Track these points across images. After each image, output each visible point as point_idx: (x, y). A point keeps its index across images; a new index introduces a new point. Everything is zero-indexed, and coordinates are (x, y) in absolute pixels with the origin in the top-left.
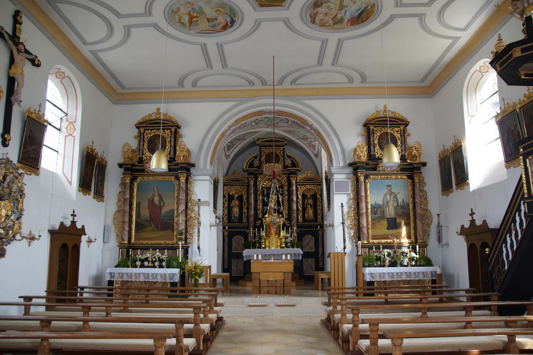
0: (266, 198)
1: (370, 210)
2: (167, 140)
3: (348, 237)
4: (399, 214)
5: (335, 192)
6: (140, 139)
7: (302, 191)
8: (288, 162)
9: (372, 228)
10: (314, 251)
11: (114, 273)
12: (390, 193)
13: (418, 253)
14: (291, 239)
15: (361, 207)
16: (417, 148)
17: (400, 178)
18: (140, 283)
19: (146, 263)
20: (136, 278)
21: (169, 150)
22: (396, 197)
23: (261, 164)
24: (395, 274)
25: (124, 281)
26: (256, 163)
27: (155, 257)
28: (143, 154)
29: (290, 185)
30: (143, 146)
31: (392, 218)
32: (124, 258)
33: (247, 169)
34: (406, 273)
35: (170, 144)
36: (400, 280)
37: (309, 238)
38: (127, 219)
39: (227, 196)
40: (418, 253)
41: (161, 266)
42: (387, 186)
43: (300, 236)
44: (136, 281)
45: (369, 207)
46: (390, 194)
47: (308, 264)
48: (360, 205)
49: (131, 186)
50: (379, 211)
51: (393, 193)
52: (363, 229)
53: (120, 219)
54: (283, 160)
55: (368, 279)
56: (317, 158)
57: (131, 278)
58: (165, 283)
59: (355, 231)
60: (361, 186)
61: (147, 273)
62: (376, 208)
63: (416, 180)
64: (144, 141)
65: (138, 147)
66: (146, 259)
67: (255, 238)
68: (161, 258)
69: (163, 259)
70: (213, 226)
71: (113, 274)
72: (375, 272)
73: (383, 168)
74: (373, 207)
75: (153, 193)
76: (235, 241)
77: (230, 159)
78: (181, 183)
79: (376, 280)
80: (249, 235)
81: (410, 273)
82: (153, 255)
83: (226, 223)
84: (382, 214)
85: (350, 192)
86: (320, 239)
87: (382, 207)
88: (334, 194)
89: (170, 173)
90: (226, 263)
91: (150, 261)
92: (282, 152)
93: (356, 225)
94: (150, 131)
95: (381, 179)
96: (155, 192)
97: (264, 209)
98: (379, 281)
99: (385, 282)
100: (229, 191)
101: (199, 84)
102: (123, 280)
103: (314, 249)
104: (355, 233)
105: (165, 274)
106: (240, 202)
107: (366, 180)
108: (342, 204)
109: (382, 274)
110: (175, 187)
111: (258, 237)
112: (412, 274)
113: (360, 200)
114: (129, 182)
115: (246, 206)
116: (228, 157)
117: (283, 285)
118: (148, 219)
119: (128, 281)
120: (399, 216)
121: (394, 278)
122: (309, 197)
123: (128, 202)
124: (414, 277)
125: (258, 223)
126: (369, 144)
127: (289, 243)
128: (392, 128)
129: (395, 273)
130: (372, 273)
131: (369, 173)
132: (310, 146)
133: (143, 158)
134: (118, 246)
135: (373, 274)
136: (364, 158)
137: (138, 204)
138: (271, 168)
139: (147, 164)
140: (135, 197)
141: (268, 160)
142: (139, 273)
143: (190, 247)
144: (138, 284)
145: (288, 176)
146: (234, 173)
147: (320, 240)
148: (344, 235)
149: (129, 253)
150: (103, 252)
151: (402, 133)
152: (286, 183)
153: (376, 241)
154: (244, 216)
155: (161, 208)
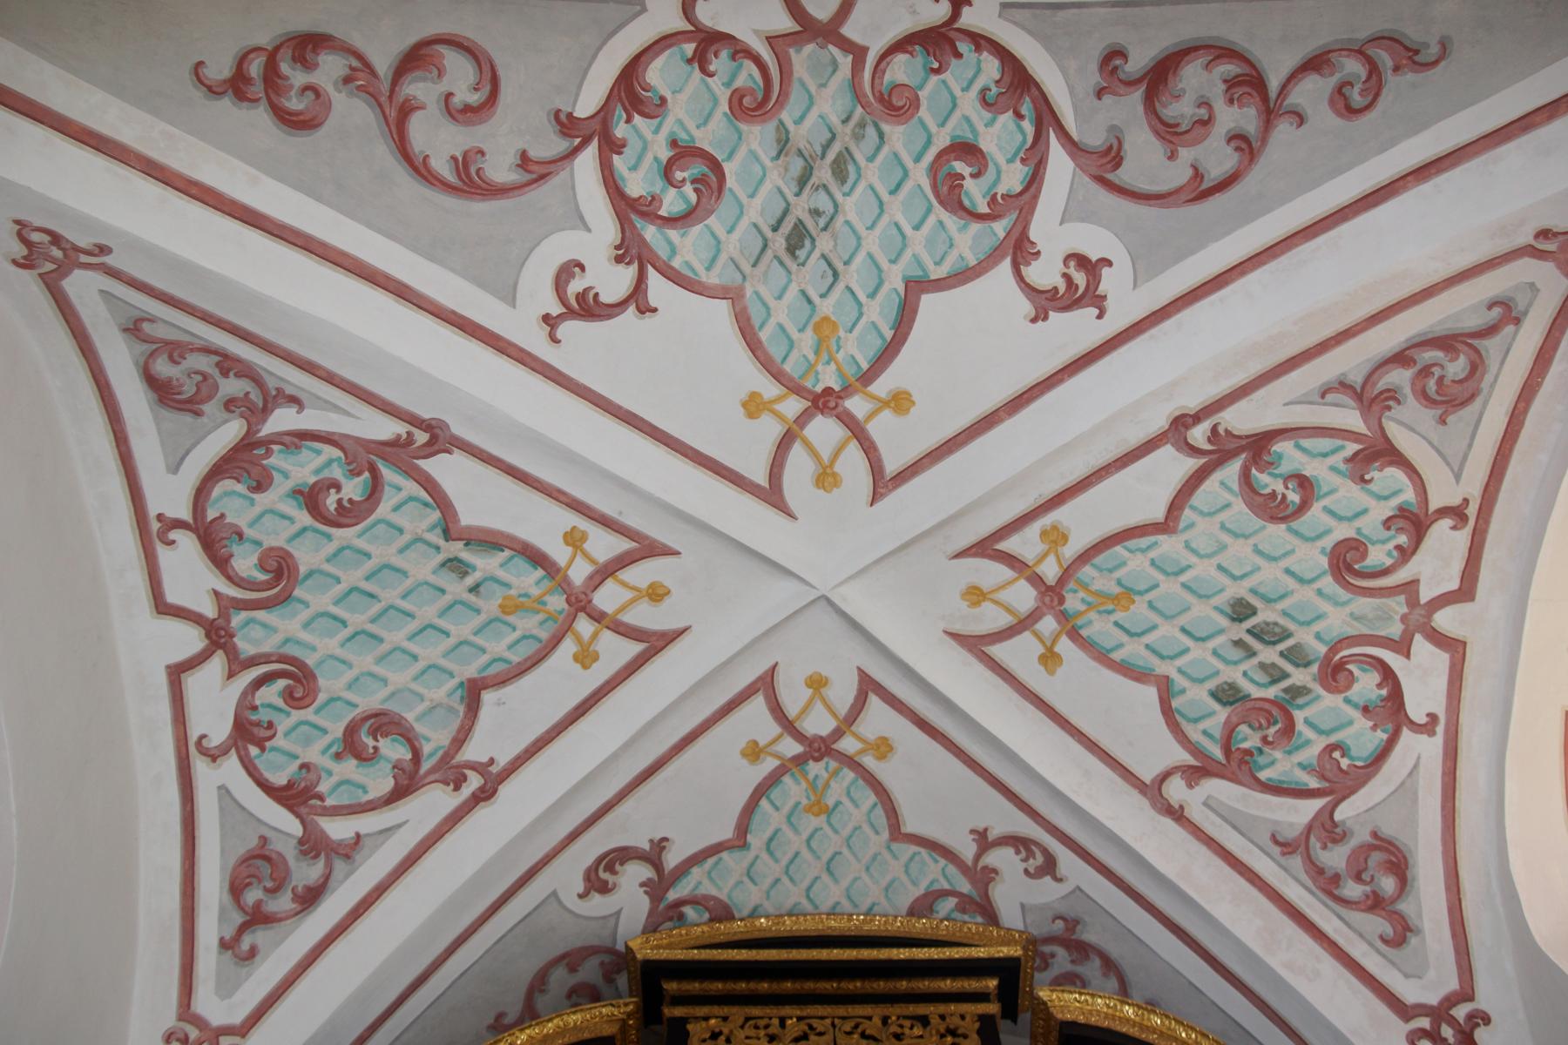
132: (1327, 883)
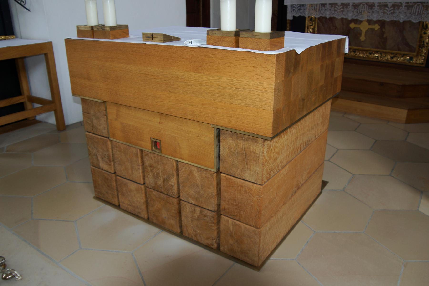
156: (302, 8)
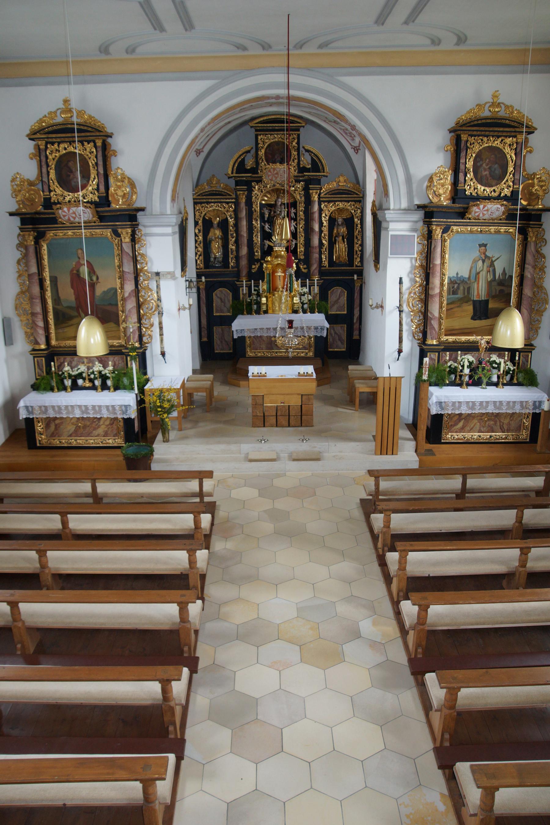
0: (267, 226)
1: (446, 287)
2: (91, 164)
3: (407, 331)
4: (493, 294)
5: (389, 255)
6: (40, 161)
7: (330, 213)
8: (306, 161)
9: (447, 318)
10: (345, 312)
11: (32, 407)
12: (484, 258)
13: (517, 364)
14: (310, 297)
15: (433, 284)
16: (542, 181)
17: (505, 232)
18: (76, 419)
19: (80, 382)
20: (68, 413)
21: (96, 180)
22: (492, 264)
23: (257, 163)
24: (478, 404)
25: (49, 417)
26: (250, 163)
27: (93, 373)
28: (50, 191)
29: (308, 202)
30: (48, 175)
31: (482, 300)
32: (43, 372)
33: (235, 175)
34: (495, 402)
35: (97, 170)
36: (484, 412)
37: (339, 291)
38: (38, 309)
39: (200, 222)
40: (517, 364)
41: (105, 387)
42: (480, 246)
43: (324, 295)
44: (69, 417)
45: (446, 281)
46: (482, 260)
47: (335, 333)
48: (431, 280)
49: (36, 248)
50: (462, 288)
51: (489, 258)
52: (432, 322)
53: (27, 307)
54: (296, 157)
55: (434, 411)
56: (357, 153)
57: (60, 413)
58: (116, 419)
59: (418, 321)
60: (435, 247)
61: (84, 406)
62: (456, 283)
63: (532, 238)
64: (48, 166)
65: (38, 175)
66: (80, 376)
67: (250, 296)
68: (103, 373)
69: (108, 375)
70: (184, 309)
71: (30, 409)
72: (446, 401)
73: (477, 214)
74: (452, 282)
75: (77, 259)
76: (218, 297)
77: (203, 155)
78: (124, 245)
79: (446, 412)
80: (241, 289)
81: (501, 402)
82: (88, 369)
83: (201, 269)
84: (466, 294)
85: (416, 256)
86: (356, 295)
87: (466, 282)
88: (386, 257)
89: (102, 224)
90: (205, 333)
91: (87, 379)
92: (296, 141)
93: (420, 311)
94: (56, 145)
95: (471, 232)
96: (79, 258)
97: (264, 245)
98: (452, 413)
99: (460, 415)
100: (204, 213)
101: (139, 50)
102: (48, 416)
103: (346, 309)
104: (419, 324)
105: (113, 406)
106: (223, 233)
107: (445, 235)
108: (401, 279)
109: (457, 404)
110: (114, 248)
111: (256, 293)
112: (504, 404)
113: (431, 271)
114: (33, 243)
115: (234, 239)
116: (199, 153)
117: (300, 414)
118: (74, 304)
119: (56, 417)
120: (493, 297)
121: (475, 409)
122: (340, 223)
123: (36, 279)
124: (506, 409)
125: (255, 267)
126: (456, 171)
127: (306, 303)
128: (503, 138)
129: (478, 402)
130: (442, 402)
131: (451, 222)
132: (346, 134)
133: (50, 198)
134: (31, 354)
135: (443, 403)
136: (445, 201)
137: (54, 280)
138: (275, 172)
139: (60, 211)
140: (47, 269)
141: (270, 156)
142: (72, 406)
143: (149, 348)
144: (72, 421)
145: (305, 185)
146: (209, 182)
147: (356, 295)
148: (401, 331)
149: (51, 369)
150: (7, 361)
151: (518, 150)
152: (301, 198)
153: (451, 339)
154: (231, 256)
155: (93, 286)
156: (243, 331)
